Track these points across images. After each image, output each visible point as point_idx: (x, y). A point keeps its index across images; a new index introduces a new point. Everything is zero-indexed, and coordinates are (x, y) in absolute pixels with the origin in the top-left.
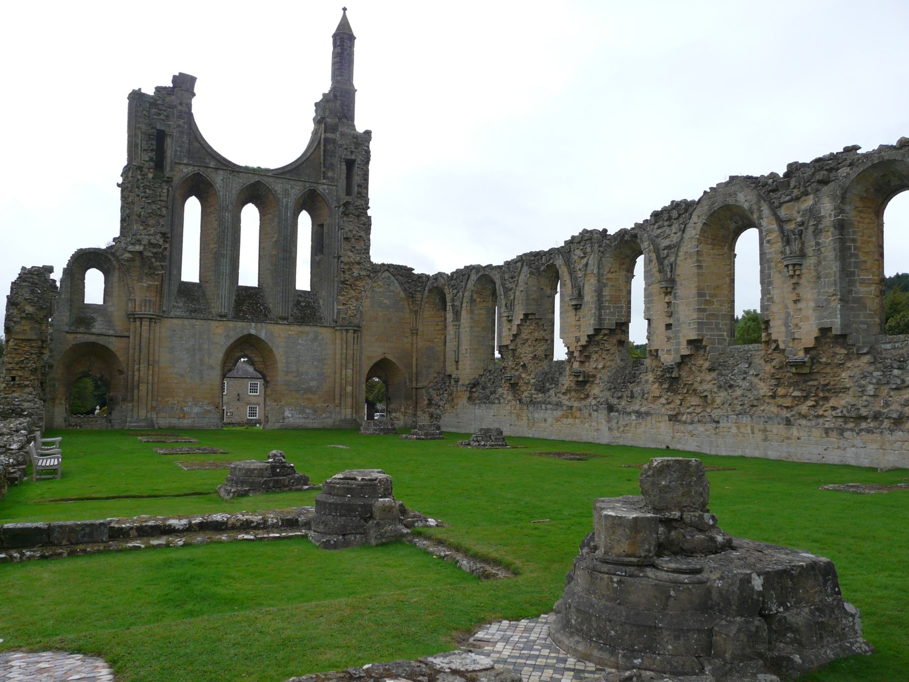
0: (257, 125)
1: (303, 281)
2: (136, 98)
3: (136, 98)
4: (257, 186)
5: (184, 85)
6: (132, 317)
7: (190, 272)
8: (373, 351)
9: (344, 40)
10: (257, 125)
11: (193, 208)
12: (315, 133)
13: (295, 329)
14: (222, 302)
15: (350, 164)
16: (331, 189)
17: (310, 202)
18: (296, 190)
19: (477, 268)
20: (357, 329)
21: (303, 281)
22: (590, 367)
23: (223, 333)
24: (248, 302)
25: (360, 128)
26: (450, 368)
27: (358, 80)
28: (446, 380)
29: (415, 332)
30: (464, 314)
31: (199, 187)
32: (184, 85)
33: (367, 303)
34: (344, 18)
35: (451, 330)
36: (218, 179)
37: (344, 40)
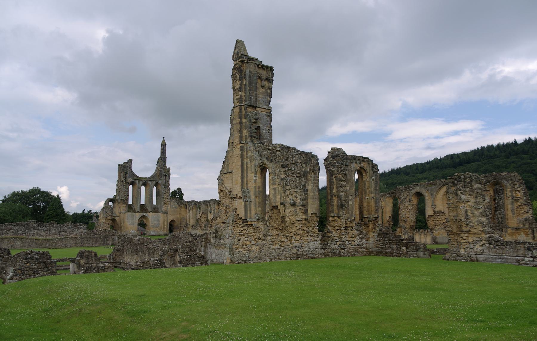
0: (145, 168)
1: (154, 203)
2: (119, 165)
3: (119, 165)
4: (145, 182)
5: (130, 161)
6: (120, 212)
7: (130, 202)
8: (171, 218)
9: (163, 146)
10: (145, 168)
11: (131, 187)
12: (157, 168)
13: (154, 214)
14: (138, 208)
15: (165, 176)
16: (162, 182)
17: (156, 185)
18: (154, 183)
19: (194, 201)
20: (167, 213)
21: (154, 203)
22: (212, 224)
23: (138, 215)
24: (143, 208)
25: (168, 166)
26: (188, 222)
27: (167, 154)
28: (187, 225)
29: (180, 213)
30: (191, 211)
31: (133, 183)
32: (130, 161)
33: (169, 207)
34: (164, 141)
35: (188, 214)
36: (137, 182)
37: (163, 146)
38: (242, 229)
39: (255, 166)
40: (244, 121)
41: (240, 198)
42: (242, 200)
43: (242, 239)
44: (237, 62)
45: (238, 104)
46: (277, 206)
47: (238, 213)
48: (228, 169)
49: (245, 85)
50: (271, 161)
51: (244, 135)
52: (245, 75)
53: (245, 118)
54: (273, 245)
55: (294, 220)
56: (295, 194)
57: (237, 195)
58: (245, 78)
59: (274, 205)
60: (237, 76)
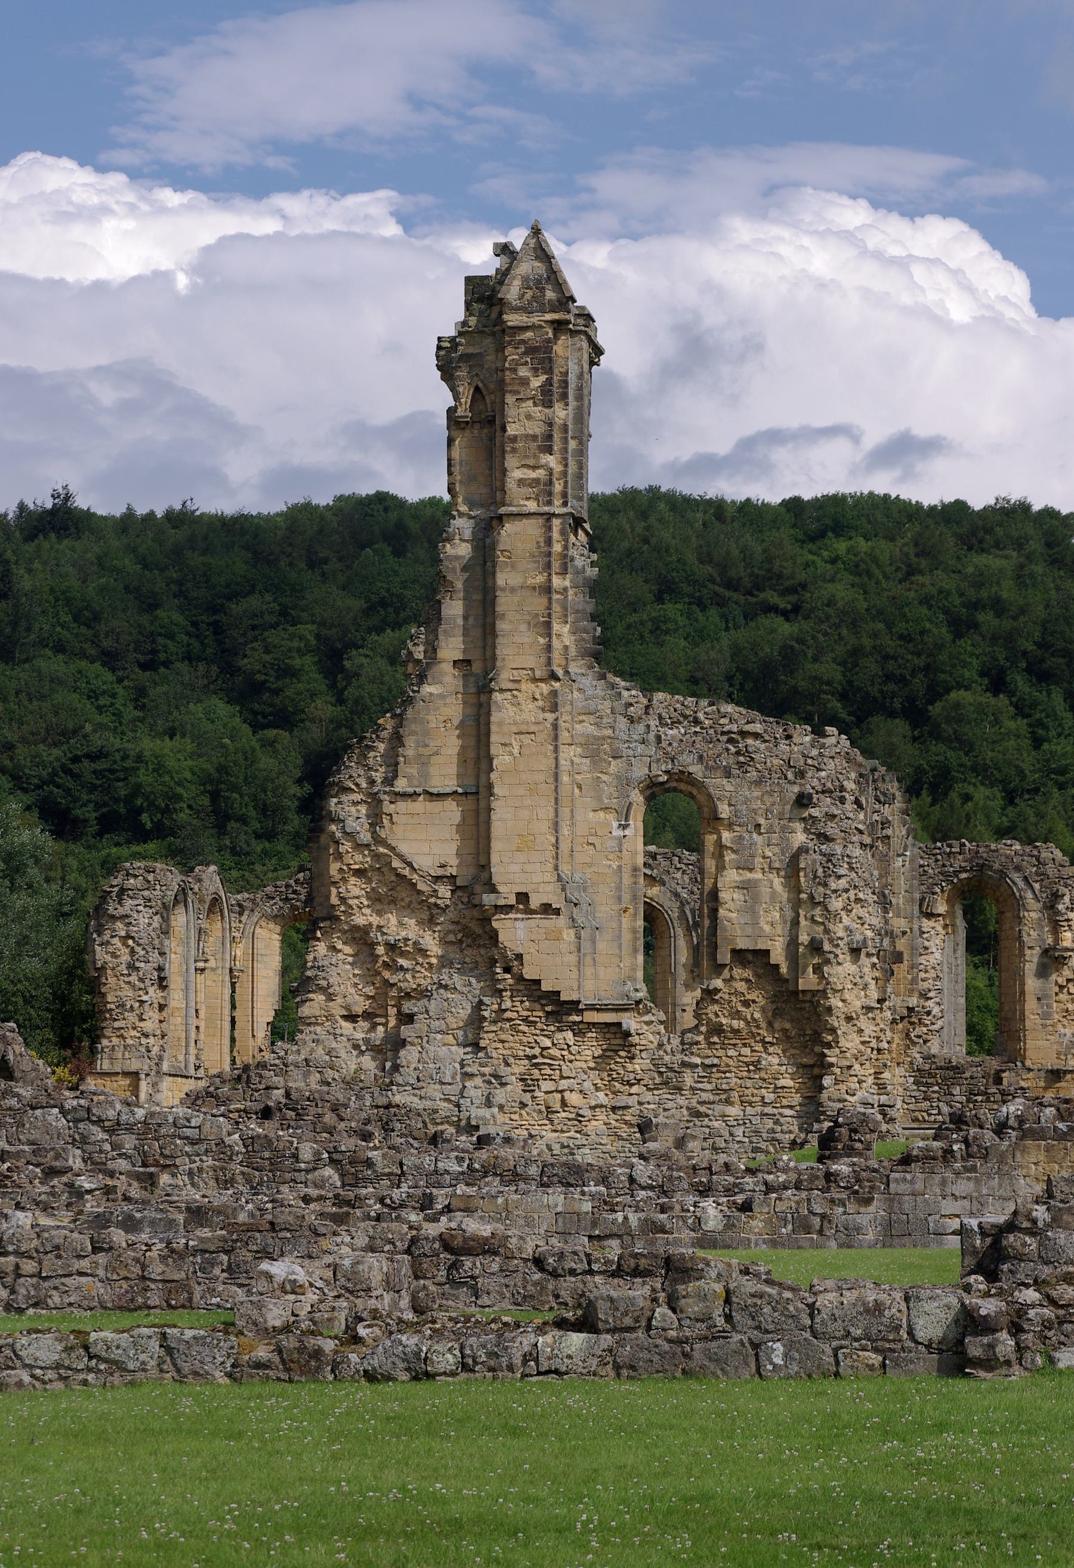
38: (547, 1043)
39: (624, 782)
40: (557, 582)
41: (547, 909)
42: (562, 921)
43: (546, 1086)
44: (535, 319)
45: (532, 506)
46: (766, 953)
47: (529, 973)
48: (425, 776)
49: (565, 428)
50: (728, 775)
51: (556, 644)
52: (565, 384)
53: (564, 572)
54: (728, 1102)
55: (858, 1004)
56: (858, 910)
57: (523, 897)
58: (564, 396)
59: (742, 944)
60: (525, 382)
